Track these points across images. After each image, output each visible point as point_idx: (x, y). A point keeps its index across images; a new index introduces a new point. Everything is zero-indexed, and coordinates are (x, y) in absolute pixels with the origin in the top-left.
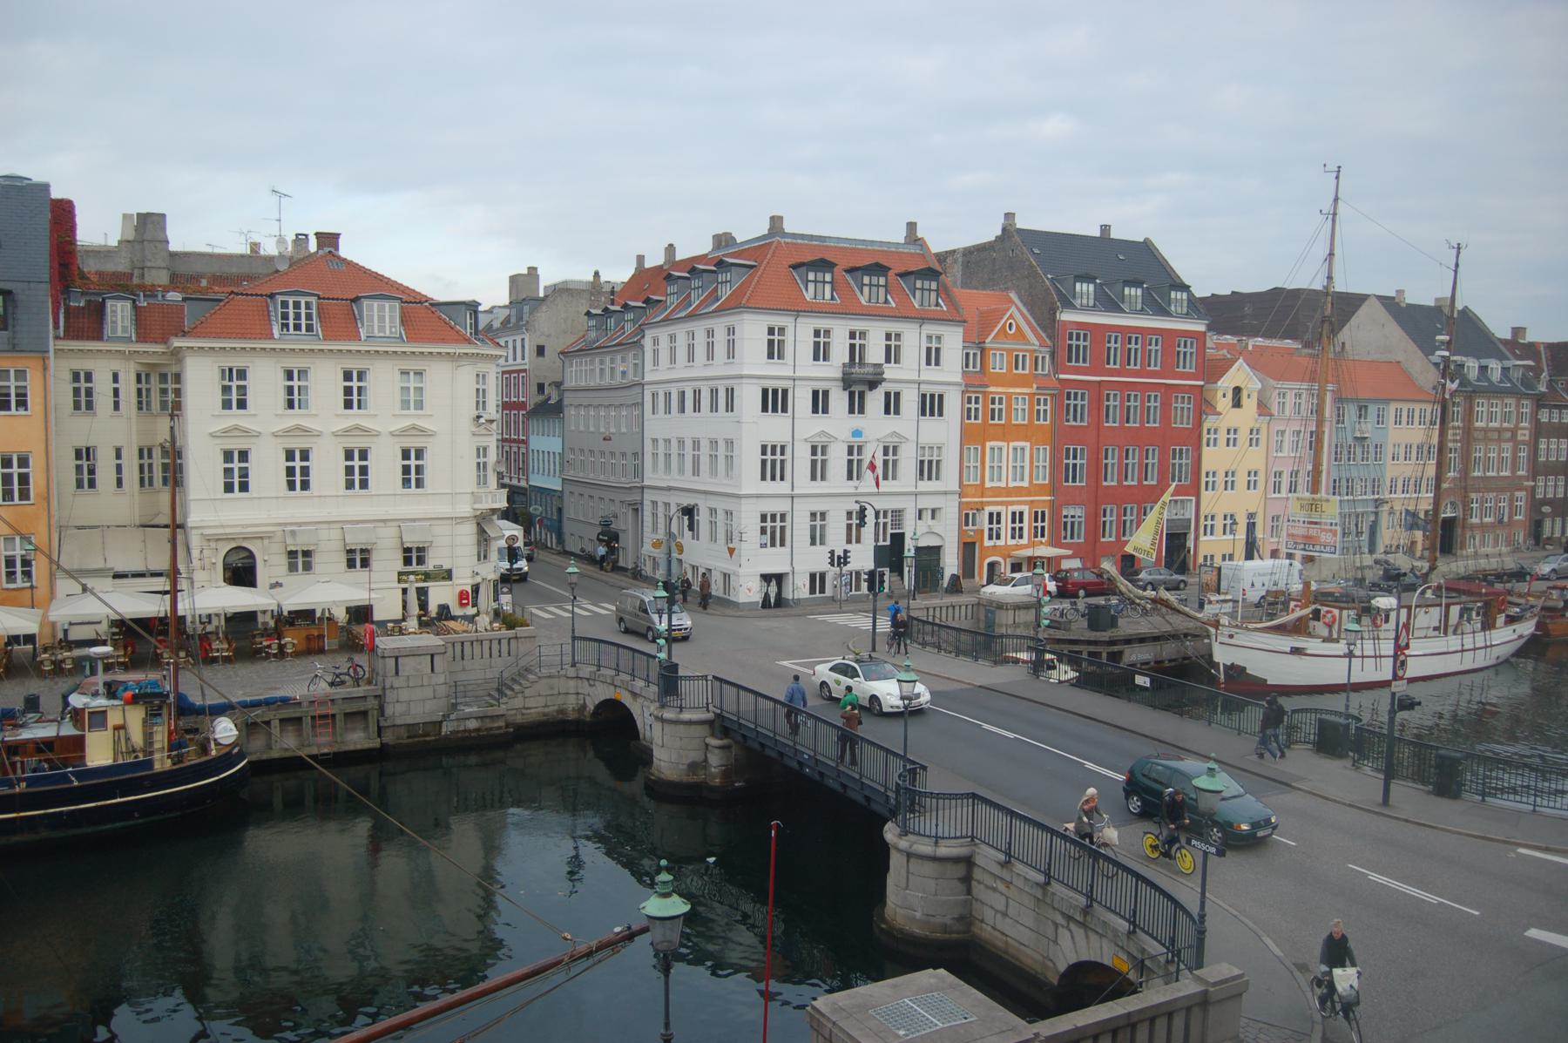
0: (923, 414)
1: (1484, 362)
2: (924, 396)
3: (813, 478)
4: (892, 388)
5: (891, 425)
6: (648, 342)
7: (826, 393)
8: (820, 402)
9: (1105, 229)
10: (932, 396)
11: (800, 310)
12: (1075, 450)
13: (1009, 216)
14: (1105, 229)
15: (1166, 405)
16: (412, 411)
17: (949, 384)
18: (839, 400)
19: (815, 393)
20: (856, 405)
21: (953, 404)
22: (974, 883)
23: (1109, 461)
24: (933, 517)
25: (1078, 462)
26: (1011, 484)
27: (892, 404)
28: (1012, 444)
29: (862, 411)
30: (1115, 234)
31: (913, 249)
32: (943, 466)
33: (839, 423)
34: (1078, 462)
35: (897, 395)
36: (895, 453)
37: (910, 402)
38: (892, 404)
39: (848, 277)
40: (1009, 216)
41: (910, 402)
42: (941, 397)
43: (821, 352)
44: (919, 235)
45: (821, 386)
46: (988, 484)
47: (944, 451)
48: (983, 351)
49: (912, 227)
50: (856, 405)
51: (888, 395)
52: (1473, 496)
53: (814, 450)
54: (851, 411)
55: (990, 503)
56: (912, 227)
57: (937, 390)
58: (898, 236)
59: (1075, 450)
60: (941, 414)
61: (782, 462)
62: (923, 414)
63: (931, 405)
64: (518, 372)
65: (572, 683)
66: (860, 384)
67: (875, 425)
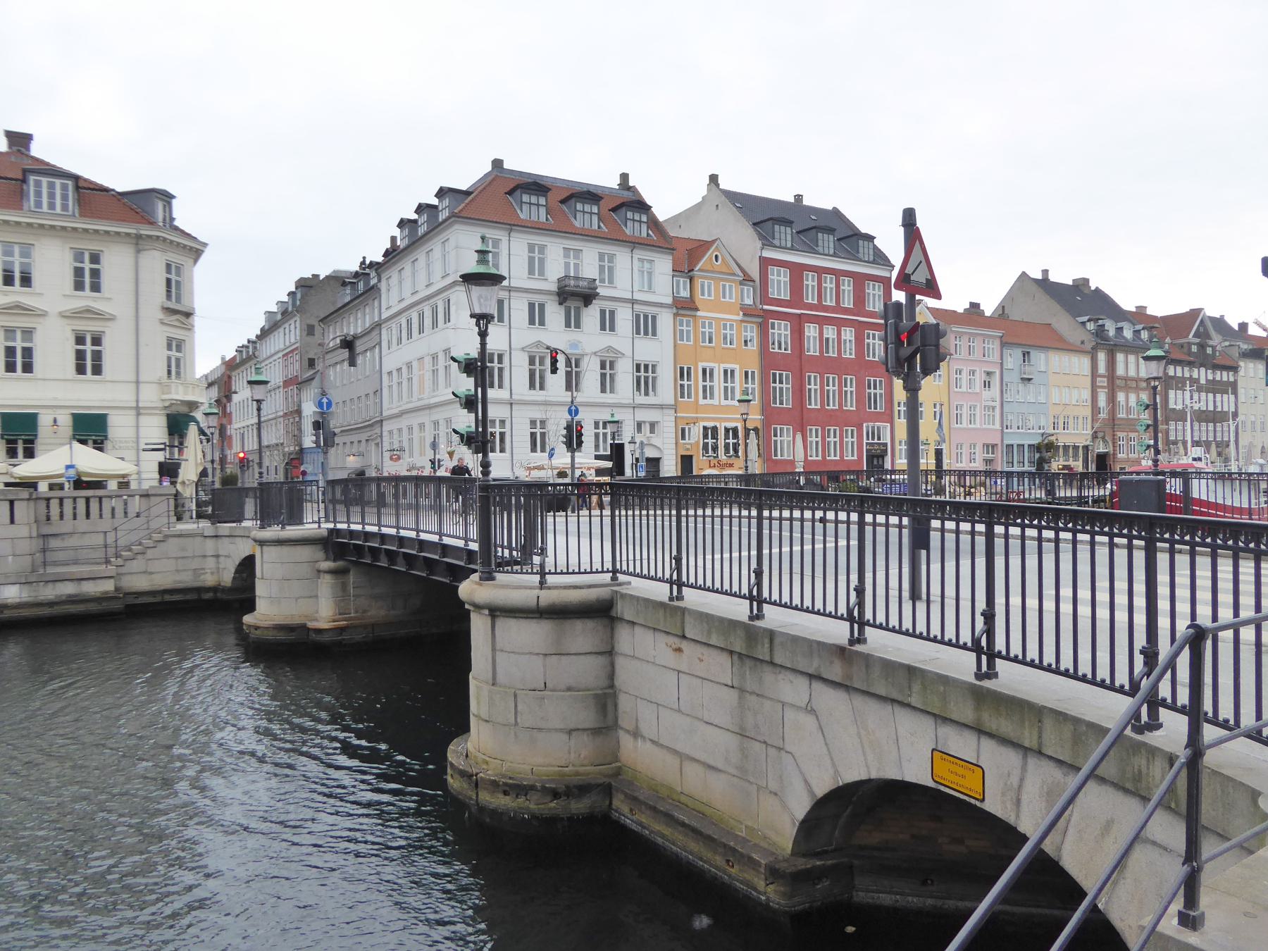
0: (638, 333)
1: (1120, 325)
2: (638, 317)
3: (532, 386)
4: (608, 305)
5: (606, 340)
6: (383, 286)
7: (542, 306)
8: (536, 316)
9: (799, 198)
10: (646, 317)
11: (514, 225)
12: (781, 375)
13: (714, 179)
14: (799, 198)
15: (859, 340)
16: (87, 292)
17: (661, 305)
18: (554, 314)
19: (531, 306)
20: (573, 321)
21: (665, 321)
22: (620, 662)
23: (812, 387)
24: (652, 431)
25: (784, 386)
26: (724, 402)
27: (608, 322)
28: (723, 366)
29: (578, 326)
30: (806, 202)
31: (626, 193)
32: (659, 383)
33: (555, 333)
34: (784, 386)
35: (612, 313)
36: (612, 367)
37: (624, 318)
38: (608, 322)
39: (564, 207)
40: (714, 179)
41: (624, 318)
42: (654, 318)
43: (536, 266)
44: (631, 184)
45: (537, 299)
46: (702, 402)
47: (658, 369)
48: (691, 279)
49: (624, 177)
50: (573, 321)
51: (603, 312)
52: (1120, 434)
53: (532, 362)
54: (568, 325)
55: (704, 419)
56: (624, 177)
57: (650, 310)
58: (613, 182)
59: (781, 375)
60: (654, 334)
61: (501, 370)
62: (638, 333)
63: (645, 326)
64: (292, 351)
65: (210, 543)
66: (576, 296)
67: (589, 338)
